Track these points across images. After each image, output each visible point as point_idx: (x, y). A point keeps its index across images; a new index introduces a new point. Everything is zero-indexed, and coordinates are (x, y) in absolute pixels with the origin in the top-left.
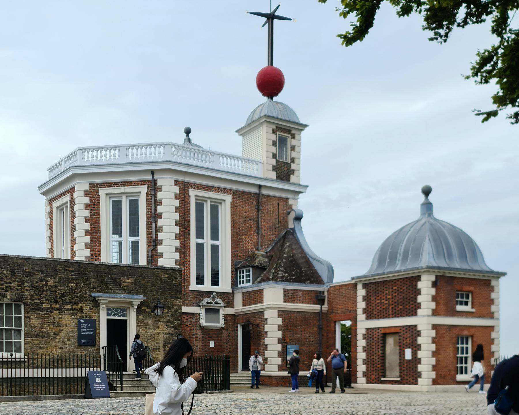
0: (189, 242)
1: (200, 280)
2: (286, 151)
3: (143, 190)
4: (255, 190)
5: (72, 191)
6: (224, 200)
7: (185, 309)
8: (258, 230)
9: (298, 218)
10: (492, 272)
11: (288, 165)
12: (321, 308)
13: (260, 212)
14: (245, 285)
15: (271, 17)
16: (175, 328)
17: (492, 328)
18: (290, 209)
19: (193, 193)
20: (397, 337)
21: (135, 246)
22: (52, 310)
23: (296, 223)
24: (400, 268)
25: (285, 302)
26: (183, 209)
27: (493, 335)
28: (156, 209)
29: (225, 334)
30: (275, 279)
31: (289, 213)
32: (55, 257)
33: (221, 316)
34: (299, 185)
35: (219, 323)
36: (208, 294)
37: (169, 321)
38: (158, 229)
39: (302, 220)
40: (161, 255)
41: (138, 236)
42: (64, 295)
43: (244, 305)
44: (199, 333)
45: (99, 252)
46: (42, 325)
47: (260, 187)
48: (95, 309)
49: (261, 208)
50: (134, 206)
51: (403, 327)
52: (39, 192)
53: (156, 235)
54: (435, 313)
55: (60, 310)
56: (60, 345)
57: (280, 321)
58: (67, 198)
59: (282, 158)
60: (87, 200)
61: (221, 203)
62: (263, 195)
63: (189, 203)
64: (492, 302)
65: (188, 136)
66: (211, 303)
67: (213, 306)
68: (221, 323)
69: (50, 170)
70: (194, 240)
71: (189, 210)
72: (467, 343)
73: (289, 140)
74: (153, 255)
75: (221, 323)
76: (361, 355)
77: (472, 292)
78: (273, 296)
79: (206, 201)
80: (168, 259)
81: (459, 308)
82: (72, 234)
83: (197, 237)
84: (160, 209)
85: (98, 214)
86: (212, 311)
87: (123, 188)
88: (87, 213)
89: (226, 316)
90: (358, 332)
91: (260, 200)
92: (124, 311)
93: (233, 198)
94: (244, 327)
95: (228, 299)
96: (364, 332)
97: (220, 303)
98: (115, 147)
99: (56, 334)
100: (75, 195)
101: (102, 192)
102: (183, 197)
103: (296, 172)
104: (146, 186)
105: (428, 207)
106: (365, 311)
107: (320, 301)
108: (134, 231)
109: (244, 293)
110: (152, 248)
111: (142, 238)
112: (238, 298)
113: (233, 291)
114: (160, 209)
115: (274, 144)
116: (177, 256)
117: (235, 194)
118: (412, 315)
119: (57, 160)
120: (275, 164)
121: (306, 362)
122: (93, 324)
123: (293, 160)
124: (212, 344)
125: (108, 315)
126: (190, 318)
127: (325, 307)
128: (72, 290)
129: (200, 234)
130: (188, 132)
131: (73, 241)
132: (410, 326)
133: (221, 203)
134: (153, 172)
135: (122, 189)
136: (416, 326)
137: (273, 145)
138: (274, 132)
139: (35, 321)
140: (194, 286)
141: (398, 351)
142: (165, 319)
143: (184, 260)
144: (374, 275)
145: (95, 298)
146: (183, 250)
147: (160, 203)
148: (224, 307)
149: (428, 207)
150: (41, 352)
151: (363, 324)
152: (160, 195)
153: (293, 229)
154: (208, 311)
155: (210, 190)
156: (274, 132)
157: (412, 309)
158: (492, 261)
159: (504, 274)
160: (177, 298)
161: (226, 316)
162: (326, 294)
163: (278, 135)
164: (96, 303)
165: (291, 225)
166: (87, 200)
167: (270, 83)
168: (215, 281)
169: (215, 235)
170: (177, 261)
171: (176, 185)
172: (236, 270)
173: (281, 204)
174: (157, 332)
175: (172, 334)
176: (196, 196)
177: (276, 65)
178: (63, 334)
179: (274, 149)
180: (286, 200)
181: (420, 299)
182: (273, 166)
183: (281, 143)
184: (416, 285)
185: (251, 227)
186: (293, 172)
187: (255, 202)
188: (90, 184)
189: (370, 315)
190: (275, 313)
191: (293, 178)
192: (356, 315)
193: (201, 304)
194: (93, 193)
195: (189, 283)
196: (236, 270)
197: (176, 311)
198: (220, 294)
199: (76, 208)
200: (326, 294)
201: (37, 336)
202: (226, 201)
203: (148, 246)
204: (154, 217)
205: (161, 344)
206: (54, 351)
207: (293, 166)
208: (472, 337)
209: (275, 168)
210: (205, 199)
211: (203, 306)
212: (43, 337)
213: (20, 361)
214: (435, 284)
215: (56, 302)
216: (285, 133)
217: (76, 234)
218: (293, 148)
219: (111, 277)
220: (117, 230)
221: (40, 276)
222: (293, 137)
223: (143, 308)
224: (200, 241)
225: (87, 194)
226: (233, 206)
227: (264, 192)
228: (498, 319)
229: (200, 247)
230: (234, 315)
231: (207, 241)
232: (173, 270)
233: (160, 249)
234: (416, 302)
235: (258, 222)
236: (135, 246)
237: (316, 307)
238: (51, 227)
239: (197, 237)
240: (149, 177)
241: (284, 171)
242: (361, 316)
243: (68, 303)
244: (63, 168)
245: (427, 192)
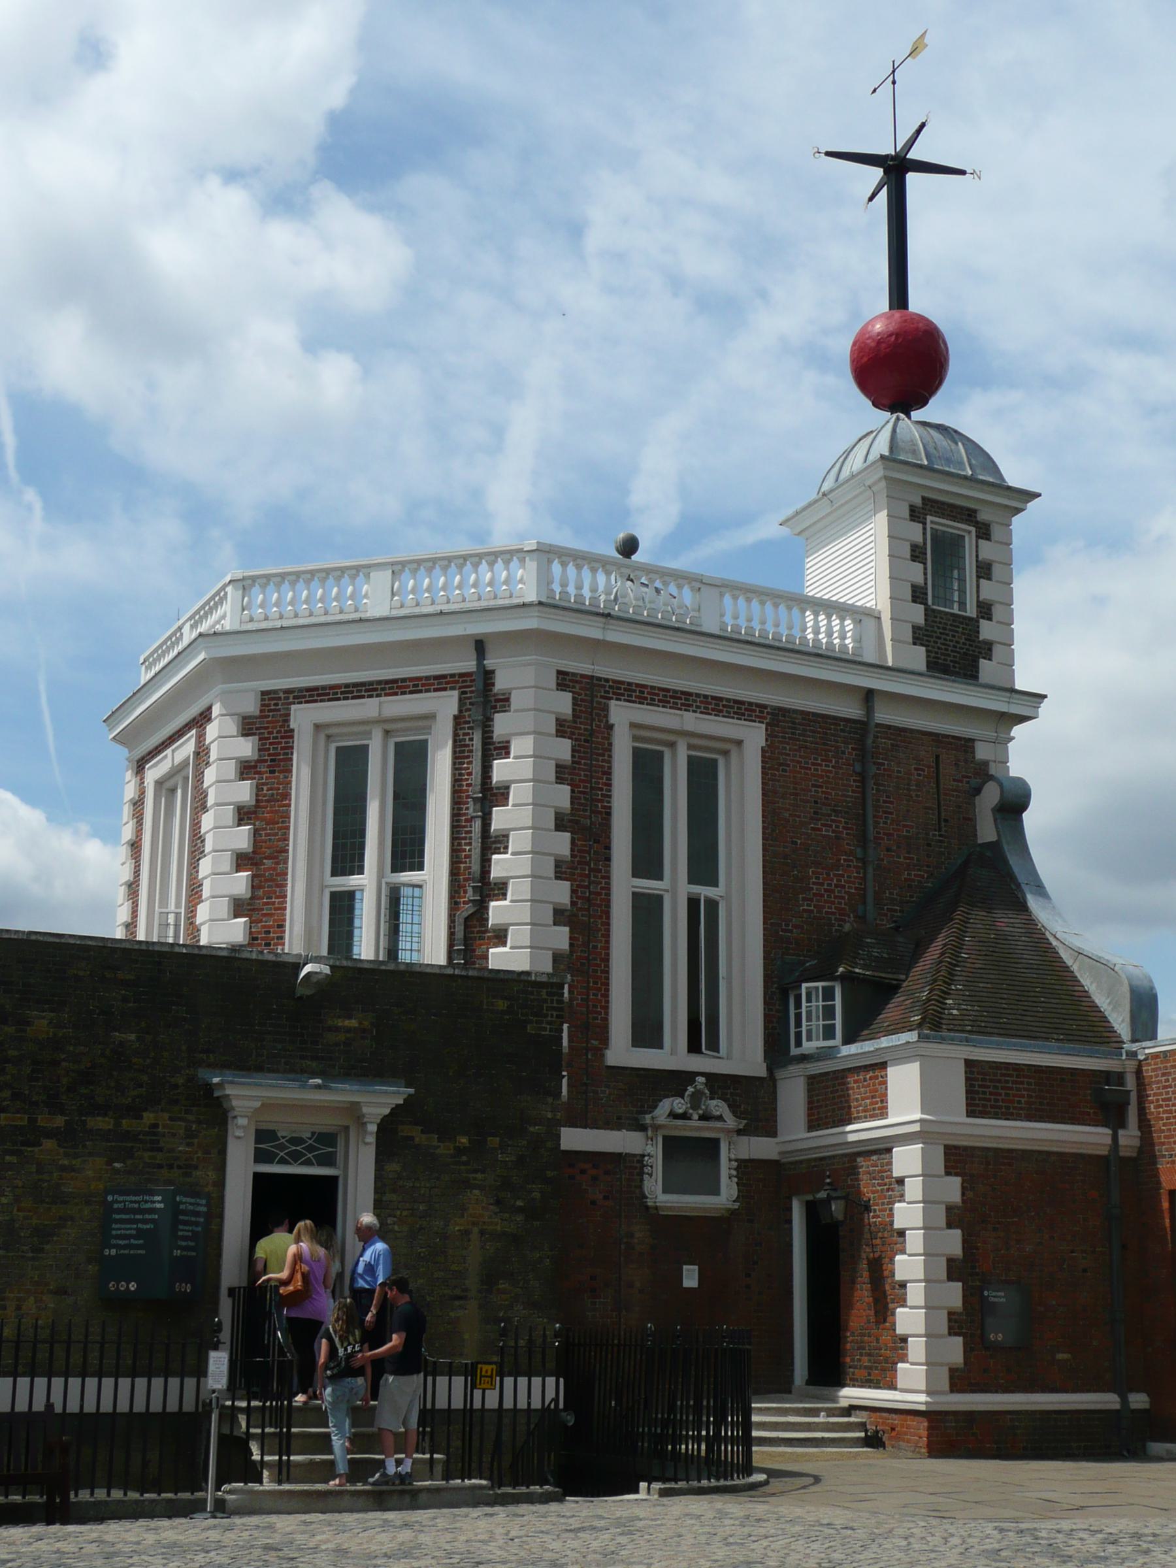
0: (608, 889)
1: (647, 1031)
2: (962, 580)
3: (446, 704)
4: (852, 710)
6: (739, 743)
8: (864, 848)
9: (1014, 804)
12: (1115, 1138)
13: (871, 783)
18: (982, 774)
19: (621, 714)
31: (978, 791)
34: (1013, 691)
35: (716, 1192)
36: (676, 1081)
38: (493, 843)
39: (1024, 815)
40: (500, 937)
41: (421, 868)
43: (811, 1128)
47: (869, 696)
49: (873, 770)
50: (411, 764)
53: (486, 863)
59: (948, 602)
60: (246, 748)
61: (726, 753)
62: (878, 725)
63: (609, 749)
66: (684, 1116)
67: (694, 1128)
68: (727, 1195)
70: (623, 884)
71: (608, 773)
74: (471, 930)
79: (672, 745)
87: (375, 701)
88: (244, 792)
89: (746, 1169)
91: (869, 741)
93: (770, 736)
94: (813, 1211)
95: (752, 1101)
97: (720, 1118)
101: (302, 718)
103: (997, 650)
104: (456, 693)
110: (467, 910)
112: (792, 1096)
113: (770, 1070)
115: (917, 553)
116: (561, 938)
117: (779, 722)
120: (920, 619)
121: (1060, 1356)
123: (985, 610)
124: (690, 1278)
126: (607, 1173)
129: (648, 861)
133: (726, 753)
137: (914, 558)
138: (916, 514)
140: (621, 1051)
146: (584, 916)
148: (740, 1132)
155: (687, 707)
161: (746, 1169)
162: (1131, 1084)
163: (929, 526)
165: (987, 832)
166: (246, 748)
169: (704, 865)
170: (557, 958)
176: (633, 725)
179: (916, 573)
182: (916, 628)
185: (837, 838)
186: (987, 650)
188: (263, 693)
193: (648, 1119)
194: (269, 727)
195: (605, 1041)
198: (720, 1084)
200: (1131, 1084)
202: (746, 744)
204: (480, 797)
207: (987, 631)
209: (920, 636)
211: (656, 1128)
216: (954, 519)
218: (984, 570)
222: (984, 532)
224: (648, 885)
225: (247, 727)
226: (772, 762)
227: (884, 715)
230: (776, 1162)
231: (675, 886)
235: (864, 823)
240: (468, 664)
241: (958, 634)
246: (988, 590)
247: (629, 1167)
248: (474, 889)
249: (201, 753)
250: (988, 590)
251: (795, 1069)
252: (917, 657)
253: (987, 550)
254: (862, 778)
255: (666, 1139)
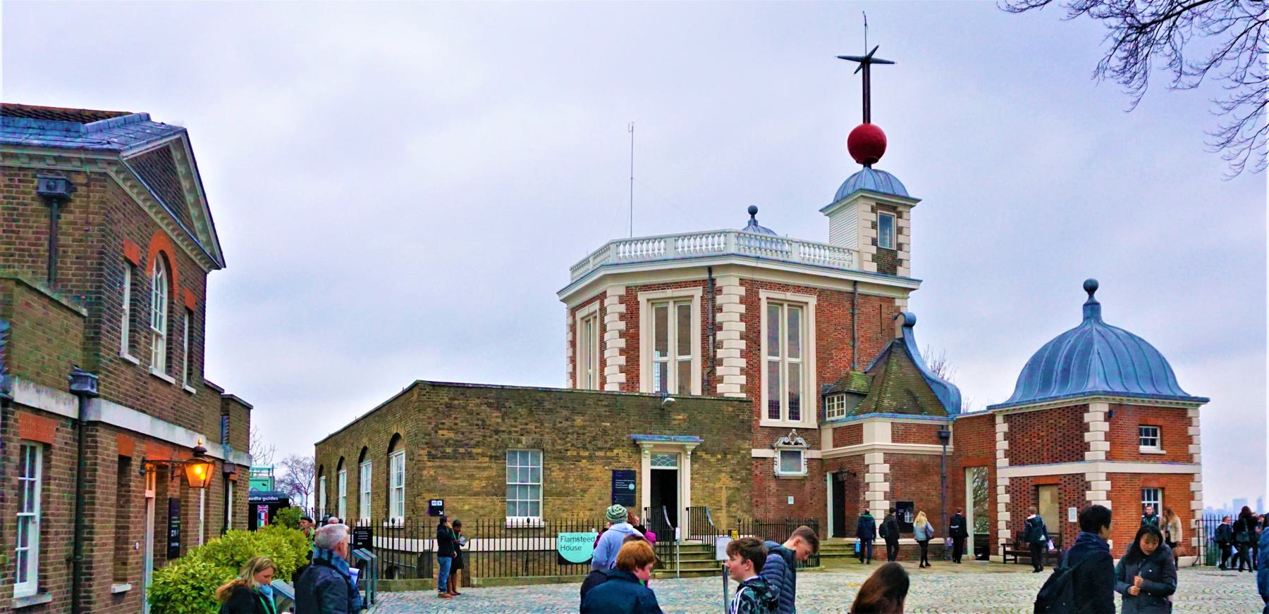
3: (698, 292)
4: (850, 289)
5: (602, 296)
7: (756, 453)
9: (909, 324)
10: (1187, 398)
11: (893, 254)
14: (836, 417)
15: (866, 63)
16: (743, 481)
17: (1190, 476)
19: (763, 294)
20: (1055, 489)
21: (685, 368)
22: (578, 459)
23: (906, 331)
24: (1059, 396)
25: (893, 441)
26: (751, 318)
27: (1193, 486)
28: (714, 317)
29: (808, 486)
30: (878, 409)
32: (578, 387)
33: (803, 461)
36: (787, 430)
37: (734, 471)
38: (717, 345)
40: (721, 380)
42: (594, 438)
43: (835, 446)
44: (773, 486)
45: (638, 376)
46: (566, 478)
48: (635, 457)
51: (1065, 476)
52: (558, 298)
54: (1110, 457)
55: (590, 458)
56: (589, 506)
57: (886, 468)
58: (596, 306)
64: (1189, 440)
65: (753, 217)
67: (792, 448)
68: (804, 471)
69: (574, 269)
70: (765, 358)
72: (1156, 499)
73: (894, 220)
74: (710, 381)
75: (804, 471)
76: (1004, 516)
77: (1161, 427)
78: (878, 434)
80: (732, 385)
81: (1144, 449)
82: (602, 353)
83: (770, 354)
84: (719, 317)
85: (637, 327)
86: (791, 455)
88: (622, 325)
90: (999, 482)
92: (675, 458)
94: (835, 477)
95: (812, 437)
96: (1007, 482)
98: (660, 239)
99: (584, 491)
100: (607, 302)
101: (642, 297)
102: (751, 302)
103: (905, 263)
105: (1092, 309)
106: (1007, 454)
107: (943, 439)
108: (684, 347)
109: (835, 429)
111: (696, 357)
112: (827, 436)
114: (719, 317)
115: (874, 226)
117: (821, 293)
118: (1078, 460)
119: (584, 256)
120: (875, 252)
122: (630, 475)
123: (900, 247)
125: (653, 463)
127: (950, 447)
128: (605, 431)
130: (753, 211)
131: (603, 363)
132: (1073, 475)
134: (710, 269)
135: (669, 293)
136: (1083, 475)
139: (557, 474)
140: (765, 421)
141: (1057, 510)
142: (729, 469)
143: (752, 386)
144: (1018, 403)
145: (635, 441)
146: (752, 372)
147: (721, 310)
149: (1092, 309)
150: (564, 515)
151: (1006, 472)
152: (720, 300)
153: (902, 340)
154: (785, 454)
156: (873, 210)
157: (1077, 451)
158: (1188, 383)
159: (1206, 401)
160: (744, 439)
164: (636, 447)
166: (622, 308)
167: (867, 145)
168: (794, 414)
169: (794, 352)
171: (741, 284)
172: (824, 397)
173: (884, 305)
174: (717, 486)
175: (738, 489)
177: (873, 122)
178: (593, 490)
179: (873, 233)
180: (891, 300)
181: (1088, 437)
183: (885, 222)
184: (1082, 418)
187: (848, 305)
189: (1015, 460)
190: (880, 457)
191: (901, 271)
192: (995, 459)
194: (630, 300)
196: (824, 397)
197: (744, 457)
198: (802, 431)
199: (607, 319)
200: (951, 429)
201: (560, 494)
203: (703, 368)
204: (711, 328)
205: (724, 504)
206: (581, 514)
207: (901, 255)
208: (1163, 489)
209: (875, 258)
210: (780, 303)
212: (568, 494)
213: (539, 528)
214: (1109, 416)
215: (585, 448)
217: (607, 354)
218: (900, 231)
219: (658, 412)
220: (662, 346)
221: (565, 413)
222: (900, 216)
223: (699, 453)
225: (622, 300)
226: (819, 309)
227: (860, 290)
228: (1199, 464)
229: (773, 367)
231: (785, 359)
232: (740, 400)
233: (720, 371)
234: (1082, 441)
236: (685, 368)
237: (938, 448)
238: (573, 344)
239: (770, 354)
240: (706, 276)
241: (889, 262)
242: (1002, 461)
243: (600, 449)
244: (590, 267)
245: (1091, 288)
246: (901, 239)
247: (772, 461)
248: (711, 362)
249: (603, 310)
250: (901, 239)
251: (828, 426)
252: (873, 267)
253: (901, 223)
254: (853, 315)
255: (782, 453)
